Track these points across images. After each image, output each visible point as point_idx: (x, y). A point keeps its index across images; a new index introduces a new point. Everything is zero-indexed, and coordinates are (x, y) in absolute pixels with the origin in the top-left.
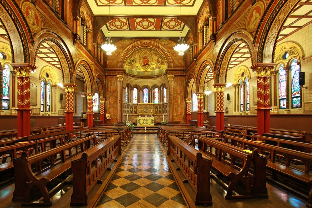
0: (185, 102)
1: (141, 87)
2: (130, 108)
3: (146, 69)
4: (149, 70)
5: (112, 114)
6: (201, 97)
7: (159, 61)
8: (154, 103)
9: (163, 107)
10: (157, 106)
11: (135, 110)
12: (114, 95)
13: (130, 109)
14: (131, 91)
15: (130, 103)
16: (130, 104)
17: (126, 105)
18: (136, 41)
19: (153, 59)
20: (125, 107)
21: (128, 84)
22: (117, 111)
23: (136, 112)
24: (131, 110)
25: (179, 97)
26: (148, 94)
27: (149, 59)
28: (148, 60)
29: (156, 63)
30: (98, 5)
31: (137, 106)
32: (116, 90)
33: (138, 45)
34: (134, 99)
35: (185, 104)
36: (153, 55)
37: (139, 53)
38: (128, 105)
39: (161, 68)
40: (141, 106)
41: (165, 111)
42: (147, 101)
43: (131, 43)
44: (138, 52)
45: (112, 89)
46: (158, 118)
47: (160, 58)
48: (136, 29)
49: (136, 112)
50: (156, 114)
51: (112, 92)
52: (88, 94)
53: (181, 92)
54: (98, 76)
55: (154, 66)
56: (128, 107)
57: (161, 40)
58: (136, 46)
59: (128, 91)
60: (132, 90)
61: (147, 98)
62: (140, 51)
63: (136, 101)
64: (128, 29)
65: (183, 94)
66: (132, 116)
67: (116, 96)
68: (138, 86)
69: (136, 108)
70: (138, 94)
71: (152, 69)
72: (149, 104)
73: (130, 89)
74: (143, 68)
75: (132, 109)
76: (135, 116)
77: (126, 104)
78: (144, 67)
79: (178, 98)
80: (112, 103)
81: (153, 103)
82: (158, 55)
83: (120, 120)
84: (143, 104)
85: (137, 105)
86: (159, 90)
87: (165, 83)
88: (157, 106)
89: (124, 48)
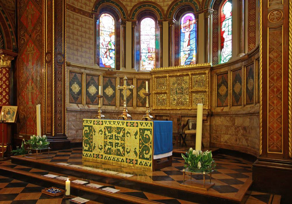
8: (215, 61)
10: (226, 73)
14: (125, 28)
15: (122, 69)
42: (194, 59)
46: (227, 127)
50: (219, 110)
61: (191, 50)
73: (120, 21)
77: (97, 73)
85: (149, 77)
88: (226, 73)
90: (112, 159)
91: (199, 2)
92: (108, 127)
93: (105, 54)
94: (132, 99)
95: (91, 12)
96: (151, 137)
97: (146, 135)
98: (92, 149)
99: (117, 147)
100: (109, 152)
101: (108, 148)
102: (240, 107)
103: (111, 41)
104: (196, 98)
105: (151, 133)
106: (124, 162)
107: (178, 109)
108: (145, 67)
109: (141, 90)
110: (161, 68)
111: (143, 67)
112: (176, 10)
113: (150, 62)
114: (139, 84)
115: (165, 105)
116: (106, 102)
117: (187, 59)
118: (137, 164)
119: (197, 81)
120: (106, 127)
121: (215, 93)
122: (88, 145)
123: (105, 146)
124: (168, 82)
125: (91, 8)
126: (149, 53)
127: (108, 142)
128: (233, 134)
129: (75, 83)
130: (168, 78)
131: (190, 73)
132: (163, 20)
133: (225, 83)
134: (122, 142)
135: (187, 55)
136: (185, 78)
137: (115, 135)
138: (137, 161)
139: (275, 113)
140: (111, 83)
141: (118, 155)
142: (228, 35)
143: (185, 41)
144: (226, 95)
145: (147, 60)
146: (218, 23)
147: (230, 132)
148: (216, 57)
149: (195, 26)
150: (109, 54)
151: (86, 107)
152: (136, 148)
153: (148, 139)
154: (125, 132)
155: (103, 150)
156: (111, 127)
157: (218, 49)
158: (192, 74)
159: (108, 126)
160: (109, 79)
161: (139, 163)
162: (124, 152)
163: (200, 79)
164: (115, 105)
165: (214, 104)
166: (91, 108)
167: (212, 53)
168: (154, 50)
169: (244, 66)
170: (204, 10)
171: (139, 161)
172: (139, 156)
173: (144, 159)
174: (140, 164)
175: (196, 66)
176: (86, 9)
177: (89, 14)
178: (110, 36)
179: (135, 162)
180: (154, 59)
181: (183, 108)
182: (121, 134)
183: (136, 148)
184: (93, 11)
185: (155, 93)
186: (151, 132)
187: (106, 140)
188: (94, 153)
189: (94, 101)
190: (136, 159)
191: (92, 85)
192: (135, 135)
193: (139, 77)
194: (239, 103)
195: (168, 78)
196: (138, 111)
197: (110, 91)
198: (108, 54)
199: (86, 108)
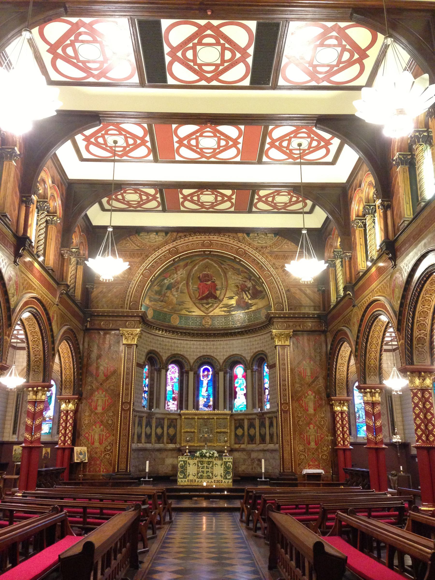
0: (328, 408)
1: (192, 361)
2: (154, 425)
3: (207, 309)
4: (218, 311)
5: (97, 444)
6: (374, 399)
7: (247, 289)
8: (231, 409)
9: (262, 425)
10: (243, 420)
11: (172, 431)
12: (106, 385)
13: (154, 428)
16: (154, 414)
18: (180, 237)
19: (230, 282)
20: (140, 424)
21: (151, 352)
22: (112, 438)
23: (172, 439)
24: (159, 431)
25: (310, 393)
27: (218, 283)
28: (214, 286)
29: (237, 294)
30: (82, 159)
32: (115, 372)
33: (185, 248)
34: (170, 395)
35: (329, 415)
36: (230, 273)
37: (189, 267)
38: (150, 416)
39: (253, 308)
40: (190, 418)
41: (268, 438)
42: (211, 403)
43: (166, 243)
44: (186, 265)
45: (102, 368)
47: (250, 280)
48: (182, 208)
49: (172, 439)
50: (237, 446)
51: (102, 377)
52: (33, 387)
53: (317, 377)
54: (65, 332)
55: (233, 302)
56: (149, 424)
57: (251, 235)
58: (181, 250)
59: (151, 372)
60: (163, 371)
61: (209, 395)
62: (191, 262)
63: (176, 402)
64: (160, 208)
65: (321, 382)
66: (159, 450)
67: (113, 390)
68: (182, 356)
69: (175, 427)
70: (181, 382)
71: (225, 309)
72: (216, 412)
74: (200, 306)
76: (170, 453)
77: (143, 415)
78: (202, 304)
79: (306, 397)
80: (99, 409)
82: (243, 272)
83: (123, 466)
84: (196, 414)
86: (249, 371)
87: (267, 351)
88: (243, 420)
89: (143, 256)
91: (219, 363)
96: (232, 466)
102: (255, 445)
108: (169, 407)
112: (200, 362)
113: (173, 402)
114: (169, 423)
117: (205, 402)
121: (233, 434)
123: (198, 474)
130: (196, 420)
131: (215, 418)
134: (212, 470)
136: (211, 420)
138: (222, 481)
141: (208, 478)
144: (243, 435)
145: (171, 401)
146: (232, 380)
147: (247, 463)
155: (196, 476)
158: (217, 418)
161: (223, 482)
164: (151, 443)
165: (233, 442)
179: (220, 482)
182: (211, 465)
184: (144, 362)
185: (184, 432)
187: (199, 470)
194: (253, 442)
195: (196, 420)
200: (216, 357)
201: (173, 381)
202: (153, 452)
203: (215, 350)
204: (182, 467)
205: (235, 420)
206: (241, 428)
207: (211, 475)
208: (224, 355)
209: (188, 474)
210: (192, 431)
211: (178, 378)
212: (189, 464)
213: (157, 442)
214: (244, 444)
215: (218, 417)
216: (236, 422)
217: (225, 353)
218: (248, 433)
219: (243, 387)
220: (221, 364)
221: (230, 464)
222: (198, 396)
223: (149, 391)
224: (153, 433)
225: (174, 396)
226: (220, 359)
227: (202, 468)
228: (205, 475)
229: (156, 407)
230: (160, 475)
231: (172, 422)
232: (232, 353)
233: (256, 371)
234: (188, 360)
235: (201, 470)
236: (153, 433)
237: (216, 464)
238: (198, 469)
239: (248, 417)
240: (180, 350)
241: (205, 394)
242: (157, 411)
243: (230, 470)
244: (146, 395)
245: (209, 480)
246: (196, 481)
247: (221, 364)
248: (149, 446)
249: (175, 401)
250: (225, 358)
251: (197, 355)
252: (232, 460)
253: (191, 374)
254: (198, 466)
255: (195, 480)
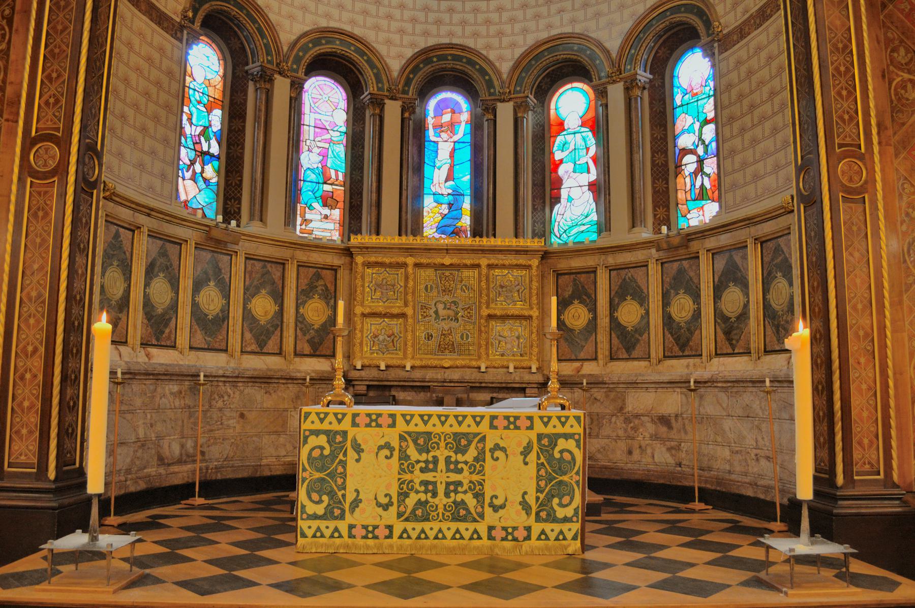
11: (315, 311)
17: (179, 243)
24: (263, 306)
26: (476, 149)
31: (334, 269)
42: (466, 221)
63: (336, 213)
66: (263, 380)
69: (330, 297)
70: (355, 143)
72: (485, 242)
73: (253, 67)
75: (278, 297)
81: (535, 244)
85: (336, 260)
90: (431, 534)
91: (498, 73)
92: (418, 434)
93: (189, 167)
94: (279, 329)
95: (178, 20)
97: (561, 452)
98: (343, 511)
99: (452, 495)
100: (422, 513)
101: (417, 500)
103: (210, 126)
104: (500, 336)
105: (578, 446)
106: (479, 538)
107: (446, 365)
109: (310, 302)
110: (374, 237)
111: (303, 227)
113: (326, 211)
114: (304, 282)
115: (397, 354)
116: (200, 339)
117: (444, 216)
118: (528, 538)
119: (502, 287)
120: (409, 433)
122: (325, 498)
123: (403, 495)
124: (411, 284)
125: (180, 8)
126: (325, 183)
127: (417, 481)
128: (617, 436)
129: (115, 263)
132: (386, 93)
133: (585, 297)
134: (475, 478)
135: (444, 206)
136: (466, 273)
137: (448, 459)
138: (528, 529)
139: (864, 387)
140: (218, 270)
141: (456, 518)
142: (574, 172)
143: (438, 164)
145: (317, 205)
146: (543, 137)
147: (606, 431)
148: (541, 224)
149: (468, 130)
150: (203, 168)
151: (141, 357)
152: (525, 493)
153: (569, 462)
154: (484, 448)
156: (429, 434)
157: (544, 202)
158: (490, 266)
159: (417, 429)
160: (213, 256)
161: (535, 535)
162: (479, 509)
163: (511, 281)
164: (226, 351)
166: (154, 361)
167: (532, 213)
168: (341, 178)
169: (657, 260)
170: (512, 96)
171: (537, 528)
172: (537, 514)
173: (555, 520)
174: (539, 539)
175: (503, 244)
176: (165, 7)
177: (173, 25)
178: (209, 111)
180: (341, 205)
181: (459, 363)
182: (472, 453)
183: (525, 493)
185: (364, 315)
186: (578, 441)
188: (354, 522)
189: (163, 332)
190: (526, 524)
191: (161, 275)
192: (522, 453)
193: (305, 259)
194: (635, 354)
195: (410, 270)
196: (299, 371)
197: (213, 300)
198: (198, 168)
199: (140, 360)
200: (484, 52)
201: (327, 137)
202: (234, 384)
203: (483, 30)
204: (320, 462)
205: (559, 274)
206: (582, 302)
207: (471, 502)
208: (513, 45)
209: (350, 497)
210: (395, 311)
211: (344, 129)
212: (358, 449)
213: (254, 347)
214: (596, 359)
215: (493, 261)
216: (563, 280)
217: (520, 39)
218: (613, 320)
219: (586, 159)
220: (505, 76)
221: (571, 444)
222: (419, 194)
223: (223, 158)
224: (236, 313)
225: (327, 188)
226: (501, 58)
227: (422, 470)
228: (441, 500)
229: (252, 217)
230: (267, 473)
231: (318, 277)
232: (544, 35)
233: (644, 88)
234: (380, 58)
235: (418, 477)
236: (236, 313)
237: (497, 447)
238: (402, 471)
239: (611, 260)
240: (353, 22)
241: (446, 189)
242: (255, 228)
243: (574, 478)
244: (210, 171)
245: (462, 526)
246: (397, 532)
247: (505, 76)
248: (213, 362)
249: (332, 208)
250: (518, 52)
251: (413, 45)
252: (578, 429)
253: (393, 110)
254: (404, 457)
255: (390, 528)
